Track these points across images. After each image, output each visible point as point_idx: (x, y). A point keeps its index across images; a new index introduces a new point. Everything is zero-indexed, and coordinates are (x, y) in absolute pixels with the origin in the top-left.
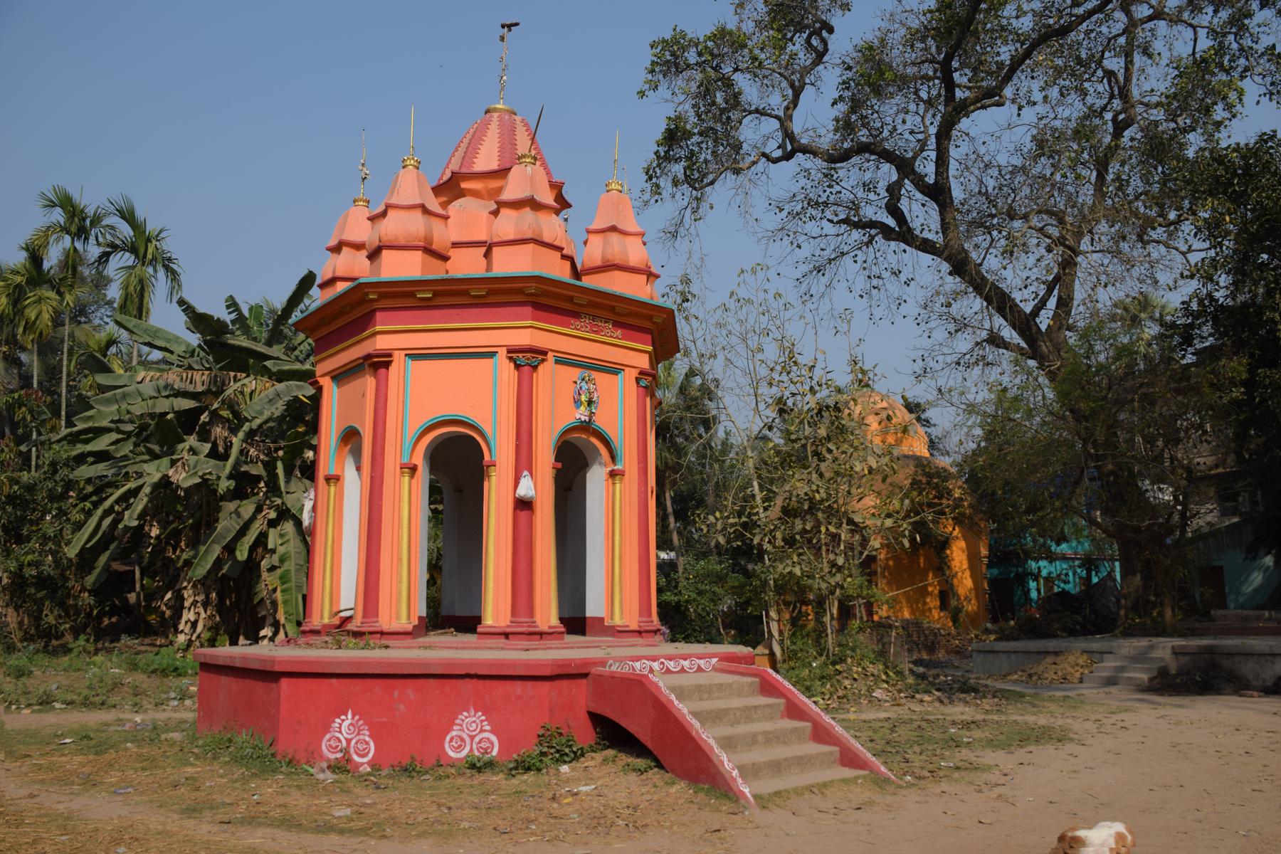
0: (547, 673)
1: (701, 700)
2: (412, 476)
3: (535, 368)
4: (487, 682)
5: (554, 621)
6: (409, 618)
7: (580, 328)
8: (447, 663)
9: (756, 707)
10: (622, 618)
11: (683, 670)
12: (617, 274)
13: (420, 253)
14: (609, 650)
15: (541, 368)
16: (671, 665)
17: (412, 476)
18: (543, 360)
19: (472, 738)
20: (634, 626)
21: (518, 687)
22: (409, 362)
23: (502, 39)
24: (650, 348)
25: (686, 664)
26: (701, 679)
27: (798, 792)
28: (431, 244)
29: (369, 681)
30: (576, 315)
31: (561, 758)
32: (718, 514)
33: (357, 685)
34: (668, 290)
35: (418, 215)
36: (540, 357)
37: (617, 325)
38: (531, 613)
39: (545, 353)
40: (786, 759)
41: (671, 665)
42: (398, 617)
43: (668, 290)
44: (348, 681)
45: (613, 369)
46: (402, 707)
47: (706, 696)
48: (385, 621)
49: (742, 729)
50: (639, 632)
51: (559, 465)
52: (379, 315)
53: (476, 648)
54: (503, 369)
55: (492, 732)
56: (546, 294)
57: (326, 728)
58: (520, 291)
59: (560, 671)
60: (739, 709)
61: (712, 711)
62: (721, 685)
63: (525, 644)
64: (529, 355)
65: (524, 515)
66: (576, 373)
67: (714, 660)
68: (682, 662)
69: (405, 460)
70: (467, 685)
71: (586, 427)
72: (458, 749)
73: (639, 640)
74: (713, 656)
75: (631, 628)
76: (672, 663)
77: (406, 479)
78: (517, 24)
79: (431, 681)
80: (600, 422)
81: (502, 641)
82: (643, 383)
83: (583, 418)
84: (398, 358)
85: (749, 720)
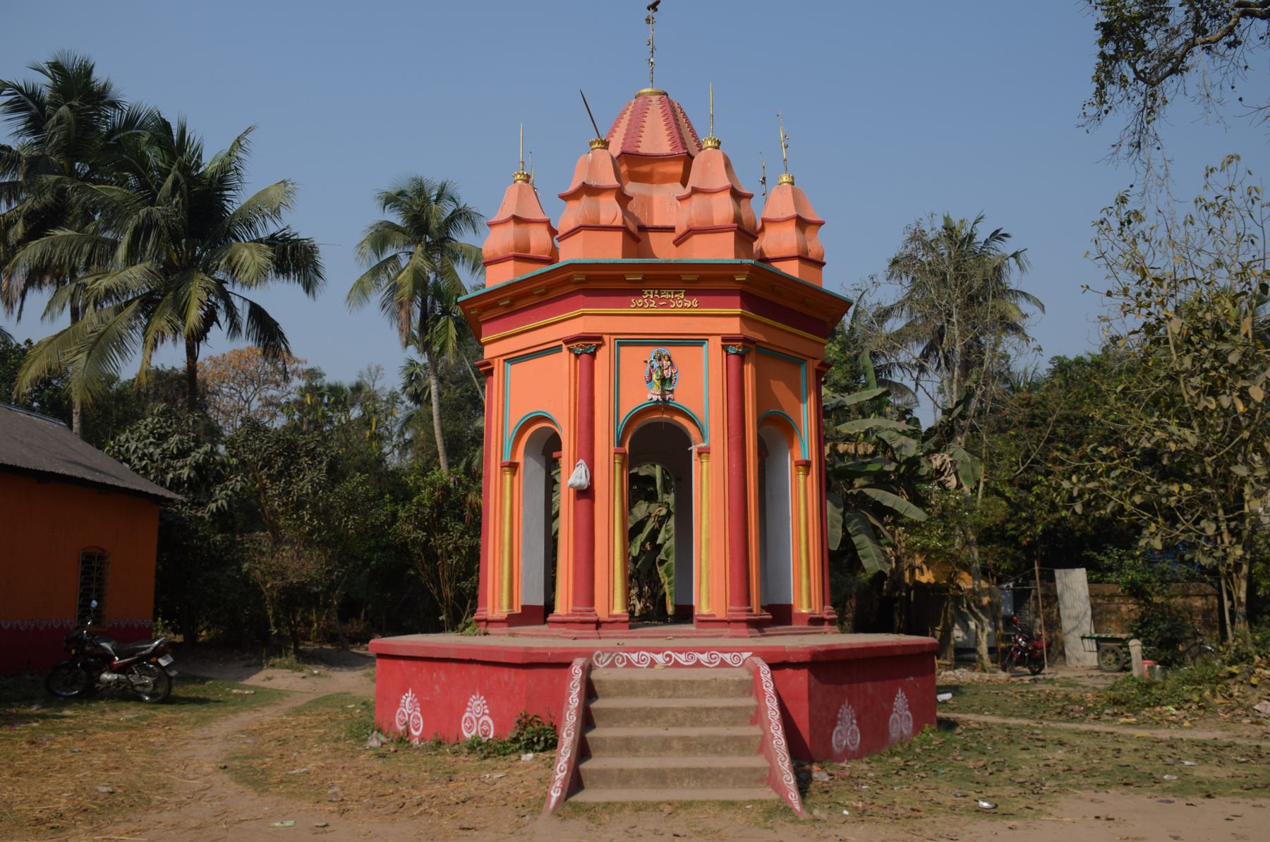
0: (519, 661)
1: (661, 696)
2: (513, 474)
3: (593, 355)
4: (487, 669)
5: (618, 609)
6: (511, 605)
7: (647, 302)
8: (528, 651)
9: (708, 710)
10: (810, 606)
11: (698, 664)
12: (695, 237)
13: (512, 262)
14: (620, 641)
15: (599, 354)
16: (682, 658)
17: (513, 474)
18: (599, 347)
19: (478, 719)
20: (721, 615)
21: (506, 675)
22: (508, 366)
23: (648, 20)
24: (738, 311)
25: (704, 658)
26: (696, 675)
27: (639, 807)
28: (528, 250)
29: (420, 664)
30: (638, 293)
31: (529, 746)
32: (1074, 478)
33: (412, 667)
34: (1104, 214)
35: (511, 225)
36: (594, 343)
37: (690, 293)
38: (591, 602)
39: (599, 338)
40: (675, 770)
41: (682, 658)
42: (500, 607)
43: (1104, 214)
44: (409, 662)
45: (696, 341)
46: (437, 687)
47: (669, 693)
48: (601, 612)
49: (694, 732)
50: (728, 622)
51: (555, 455)
52: (484, 327)
53: (544, 636)
54: (564, 360)
55: (491, 715)
56: (589, 279)
57: (397, 704)
58: (567, 281)
59: (534, 660)
60: (682, 710)
61: (639, 710)
62: (692, 682)
63: (575, 632)
64: (580, 343)
65: (584, 503)
66: (653, 351)
67: (746, 655)
68: (697, 655)
69: (507, 459)
70: (474, 670)
71: (663, 405)
72: (469, 729)
73: (728, 631)
74: (746, 649)
75: (718, 618)
76: (683, 656)
77: (508, 477)
78: (658, 3)
79: (455, 665)
80: (680, 398)
81: (591, 631)
82: (732, 350)
83: (655, 398)
84: (498, 366)
85: (696, 722)
